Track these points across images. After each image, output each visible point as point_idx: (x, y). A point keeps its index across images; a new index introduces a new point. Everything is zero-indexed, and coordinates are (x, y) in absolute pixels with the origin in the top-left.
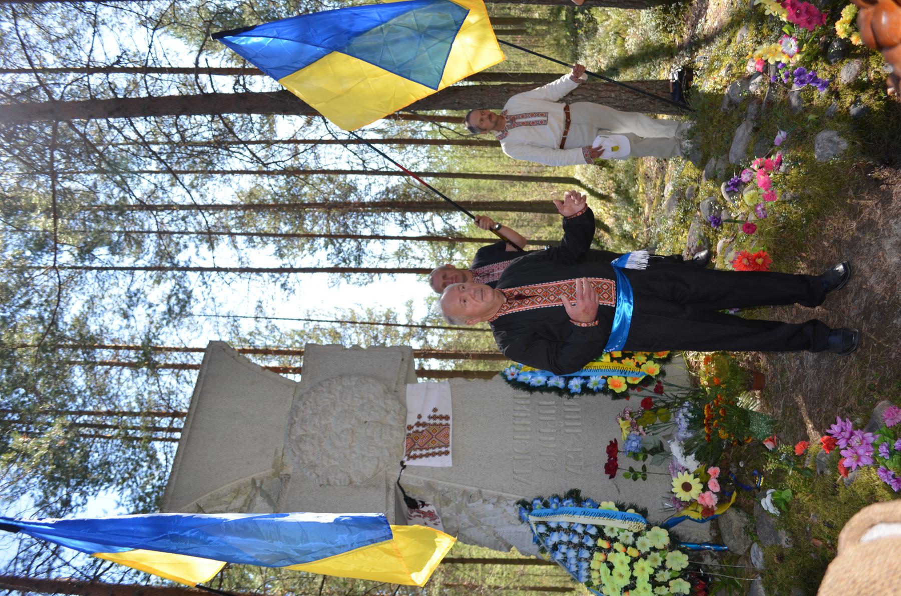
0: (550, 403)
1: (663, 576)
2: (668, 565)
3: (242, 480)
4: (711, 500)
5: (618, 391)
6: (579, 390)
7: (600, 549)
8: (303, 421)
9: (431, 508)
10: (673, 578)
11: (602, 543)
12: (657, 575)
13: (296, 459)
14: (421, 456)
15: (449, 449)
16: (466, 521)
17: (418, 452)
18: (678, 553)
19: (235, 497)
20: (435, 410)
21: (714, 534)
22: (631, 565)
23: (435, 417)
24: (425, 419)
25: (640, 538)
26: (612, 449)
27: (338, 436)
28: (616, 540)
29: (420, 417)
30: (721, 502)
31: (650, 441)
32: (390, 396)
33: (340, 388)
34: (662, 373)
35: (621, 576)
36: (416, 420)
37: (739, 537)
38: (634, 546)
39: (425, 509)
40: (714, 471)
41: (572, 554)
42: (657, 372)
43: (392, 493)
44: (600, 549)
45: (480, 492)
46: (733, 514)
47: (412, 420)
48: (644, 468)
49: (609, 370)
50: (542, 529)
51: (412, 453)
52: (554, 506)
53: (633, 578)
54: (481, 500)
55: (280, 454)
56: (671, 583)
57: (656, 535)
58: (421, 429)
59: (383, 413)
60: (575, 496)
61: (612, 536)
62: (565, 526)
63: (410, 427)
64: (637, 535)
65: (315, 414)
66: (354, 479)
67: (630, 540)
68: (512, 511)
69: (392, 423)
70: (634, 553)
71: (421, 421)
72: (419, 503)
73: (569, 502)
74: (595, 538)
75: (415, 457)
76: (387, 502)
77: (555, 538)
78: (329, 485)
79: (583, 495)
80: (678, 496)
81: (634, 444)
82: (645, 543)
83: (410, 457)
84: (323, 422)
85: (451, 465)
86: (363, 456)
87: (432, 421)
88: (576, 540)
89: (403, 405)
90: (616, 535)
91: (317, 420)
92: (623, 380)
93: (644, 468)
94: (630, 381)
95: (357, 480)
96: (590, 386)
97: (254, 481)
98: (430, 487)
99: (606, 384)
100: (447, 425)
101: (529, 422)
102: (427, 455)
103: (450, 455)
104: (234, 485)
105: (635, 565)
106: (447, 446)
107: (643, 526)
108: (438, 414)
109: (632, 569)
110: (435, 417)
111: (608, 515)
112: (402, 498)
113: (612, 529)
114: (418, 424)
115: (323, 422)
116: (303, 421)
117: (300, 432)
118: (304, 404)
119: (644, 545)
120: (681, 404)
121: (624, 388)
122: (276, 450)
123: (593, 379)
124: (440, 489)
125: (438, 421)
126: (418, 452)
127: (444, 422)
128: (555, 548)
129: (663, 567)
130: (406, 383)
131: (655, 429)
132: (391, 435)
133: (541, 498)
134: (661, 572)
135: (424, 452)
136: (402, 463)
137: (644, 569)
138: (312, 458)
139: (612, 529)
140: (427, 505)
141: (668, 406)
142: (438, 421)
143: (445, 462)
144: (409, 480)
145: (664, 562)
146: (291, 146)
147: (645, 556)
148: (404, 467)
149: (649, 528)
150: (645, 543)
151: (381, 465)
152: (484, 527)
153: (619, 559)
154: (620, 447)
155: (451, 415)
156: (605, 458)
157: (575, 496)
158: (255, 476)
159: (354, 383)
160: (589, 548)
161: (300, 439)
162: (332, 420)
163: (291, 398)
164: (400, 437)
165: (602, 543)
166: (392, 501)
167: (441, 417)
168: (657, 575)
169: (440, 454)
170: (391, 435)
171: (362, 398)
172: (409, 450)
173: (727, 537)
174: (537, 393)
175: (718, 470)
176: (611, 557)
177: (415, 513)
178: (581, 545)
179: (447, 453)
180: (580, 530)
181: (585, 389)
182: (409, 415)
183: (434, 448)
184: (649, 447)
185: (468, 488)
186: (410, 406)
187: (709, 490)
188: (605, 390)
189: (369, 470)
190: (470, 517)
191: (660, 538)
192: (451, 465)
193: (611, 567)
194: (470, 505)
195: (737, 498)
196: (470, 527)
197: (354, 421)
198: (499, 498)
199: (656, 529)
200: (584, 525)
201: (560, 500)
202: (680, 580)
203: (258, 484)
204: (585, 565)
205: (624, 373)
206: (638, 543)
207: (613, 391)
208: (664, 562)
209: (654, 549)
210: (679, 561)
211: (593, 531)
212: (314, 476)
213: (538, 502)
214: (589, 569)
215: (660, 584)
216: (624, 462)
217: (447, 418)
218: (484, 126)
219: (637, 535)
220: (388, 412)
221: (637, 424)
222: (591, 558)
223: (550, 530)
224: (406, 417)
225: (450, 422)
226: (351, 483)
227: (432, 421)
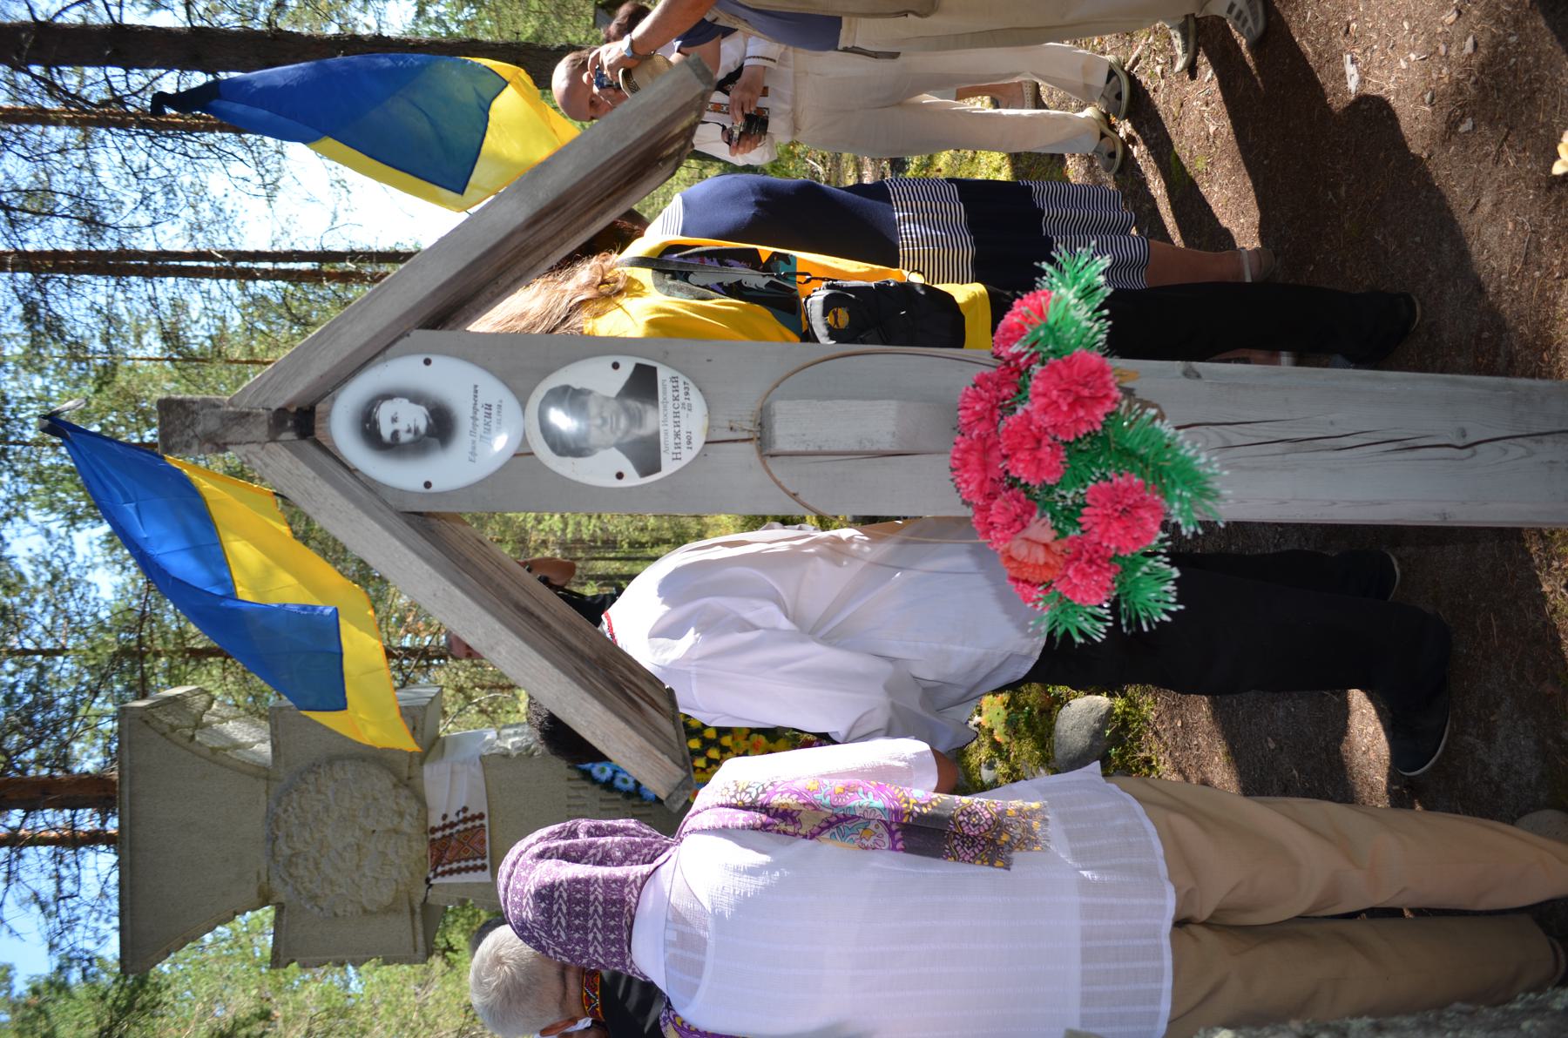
15: (487, 861)
20: (465, 809)
23: (465, 820)
24: (452, 818)
27: (340, 855)
32: (405, 792)
36: (441, 823)
51: (440, 869)
55: (264, 879)
59: (396, 820)
63: (434, 830)
65: (303, 825)
69: (409, 830)
75: (443, 874)
76: (414, 928)
86: (377, 879)
91: (307, 835)
100: (482, 826)
108: (468, 814)
110: (465, 820)
114: (444, 828)
117: (288, 852)
118: (286, 811)
122: (259, 874)
125: (469, 825)
127: (478, 823)
130: (422, 764)
132: (410, 848)
136: (428, 880)
142: (469, 825)
155: (486, 813)
159: (349, 776)
161: (290, 863)
163: (263, 797)
164: (422, 848)
167: (473, 818)
169: (475, 868)
170: (410, 848)
171: (364, 797)
172: (437, 863)
174: (597, 787)
179: (483, 868)
182: (431, 814)
183: (467, 860)
186: (430, 801)
189: (386, 895)
197: (358, 833)
212: (316, 909)
217: (481, 816)
220: (401, 815)
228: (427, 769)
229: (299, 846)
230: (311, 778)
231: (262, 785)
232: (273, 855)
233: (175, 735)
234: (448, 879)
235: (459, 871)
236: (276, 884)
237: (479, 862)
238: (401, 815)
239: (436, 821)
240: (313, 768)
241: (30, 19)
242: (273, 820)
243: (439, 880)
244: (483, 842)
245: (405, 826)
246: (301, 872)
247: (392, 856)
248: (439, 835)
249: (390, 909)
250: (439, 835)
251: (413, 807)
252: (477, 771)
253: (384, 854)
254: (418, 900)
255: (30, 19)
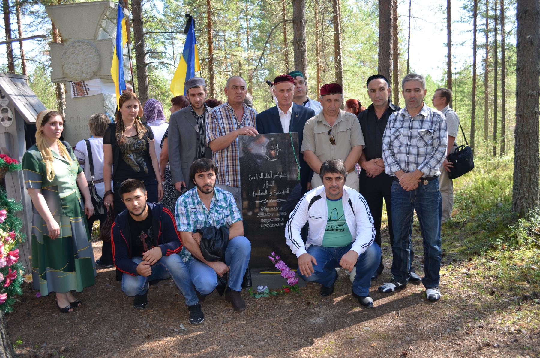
23: (86, 90)
24: (87, 87)
63: (84, 82)
65: (83, 49)
89: (91, 79)
161: (73, 46)
164: (79, 79)
169: (74, 93)
179: (75, 96)
186: (91, 81)
189: (67, 71)
217: (88, 94)
220: (87, 74)
228: (99, 79)
229: (77, 49)
230: (94, 50)
231: (92, 38)
233: (103, 15)
234: (72, 87)
235: (74, 89)
236: (69, 43)
238: (87, 74)
239: (86, 83)
240: (97, 51)
242: (83, 42)
244: (81, 95)
245: (84, 75)
246: (71, 50)
247: (76, 72)
248: (82, 84)
249: (64, 73)
250: (82, 84)
251: (89, 77)
252: (99, 93)
253: (77, 70)
254: (66, 79)
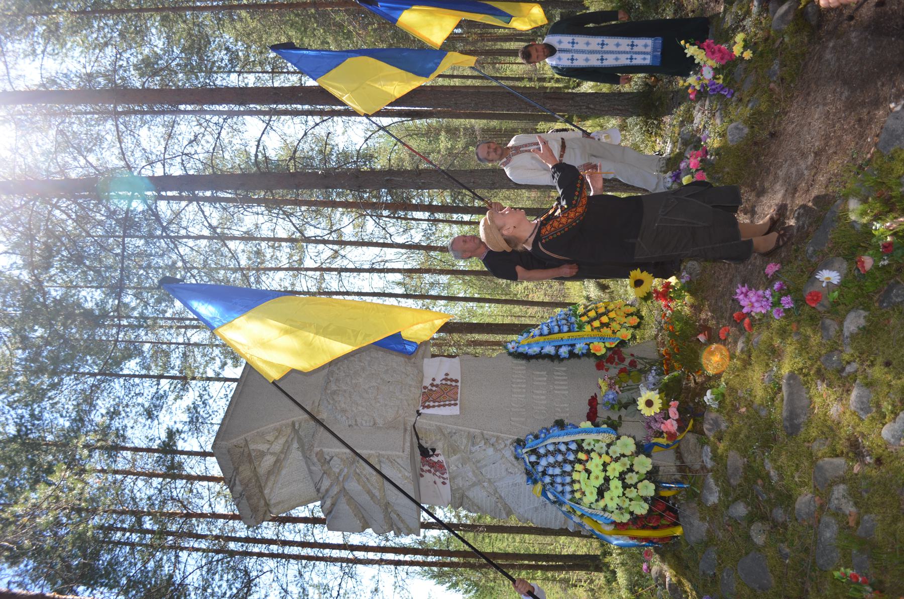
0: (542, 373)
1: (631, 478)
2: (636, 468)
3: (284, 422)
4: (671, 425)
5: (598, 354)
6: (567, 355)
7: (580, 461)
8: (337, 380)
9: (441, 458)
10: (641, 481)
11: (582, 456)
12: (627, 477)
13: (330, 407)
14: (434, 407)
15: (458, 402)
16: (470, 474)
17: (431, 404)
18: (642, 457)
19: (276, 438)
20: (447, 374)
21: (678, 463)
22: (605, 465)
23: (446, 379)
25: (612, 448)
26: (593, 402)
28: (593, 450)
29: (434, 380)
30: (681, 429)
31: (625, 397)
33: (368, 358)
34: (634, 337)
35: (597, 478)
37: (695, 451)
38: (607, 453)
39: (435, 459)
40: (674, 404)
41: (557, 471)
42: (629, 337)
43: (408, 433)
44: (580, 461)
45: (482, 434)
46: (690, 436)
47: (427, 382)
48: (620, 417)
49: (591, 338)
50: (533, 458)
51: (427, 404)
52: (543, 435)
53: (607, 479)
54: (483, 442)
56: (640, 485)
57: (626, 445)
58: (434, 388)
60: (560, 424)
61: (589, 448)
62: (551, 448)
63: (425, 388)
64: (609, 446)
66: (378, 421)
67: (605, 449)
68: (508, 453)
70: (607, 459)
71: (435, 383)
72: (431, 453)
73: (556, 431)
74: (576, 452)
75: (428, 407)
76: (404, 439)
77: (543, 462)
78: (357, 425)
79: (566, 421)
80: (642, 412)
81: (611, 396)
82: (616, 450)
83: (424, 407)
84: (354, 381)
85: (458, 413)
86: (386, 405)
87: (444, 382)
88: (560, 458)
90: (592, 446)
92: (602, 345)
93: (620, 417)
94: (608, 345)
95: (380, 422)
96: (576, 351)
97: (293, 424)
98: (440, 429)
99: (589, 349)
101: (524, 386)
102: (439, 406)
103: (458, 407)
104: (277, 424)
105: (608, 468)
106: (456, 400)
107: (614, 437)
108: (449, 377)
109: (605, 470)
110: (446, 379)
111: (587, 431)
112: (416, 445)
113: (589, 444)
114: (432, 385)
115: (354, 381)
116: (337, 380)
117: (334, 387)
118: (339, 369)
119: (615, 452)
120: (650, 370)
121: (603, 351)
123: (578, 346)
124: (449, 430)
125: (449, 383)
126: (431, 404)
127: (454, 384)
128: (544, 473)
129: (631, 470)
130: (423, 358)
131: (629, 390)
132: (410, 391)
133: (531, 434)
134: (630, 474)
135: (437, 404)
136: (418, 411)
137: (615, 469)
138: (343, 405)
139: (589, 444)
140: (437, 455)
141: (641, 371)
142: (449, 383)
143: (455, 410)
144: (421, 422)
145: (632, 465)
146: (318, 273)
147: (617, 460)
148: (419, 414)
149: (618, 438)
150: (616, 450)
151: (401, 412)
152: (485, 484)
153: (595, 464)
154: (599, 401)
156: (587, 409)
157: (560, 424)
158: (294, 419)
160: (572, 463)
162: (361, 380)
164: (418, 392)
165: (582, 456)
166: (408, 438)
167: (452, 380)
168: (627, 477)
169: (450, 405)
170: (410, 391)
173: (686, 455)
174: (533, 361)
175: (677, 403)
176: (589, 465)
177: (426, 468)
178: (565, 461)
179: (456, 404)
180: (563, 448)
181: (572, 355)
184: (624, 401)
185: (472, 430)
187: (669, 418)
188: (588, 354)
190: (474, 472)
191: (627, 445)
192: (458, 413)
193: (589, 472)
194: (473, 449)
195: (693, 426)
196: (474, 485)
198: (498, 438)
199: (624, 439)
200: (566, 444)
201: (548, 430)
202: (646, 482)
203: (297, 426)
204: (568, 479)
205: (603, 339)
206: (610, 452)
207: (594, 355)
208: (632, 465)
209: (624, 455)
210: (644, 464)
211: (573, 446)
212: (344, 418)
213: (531, 437)
214: (573, 482)
215: (630, 486)
216: (603, 413)
217: (456, 381)
218: (490, 158)
219: (609, 446)
221: (615, 384)
222: (573, 470)
223: (539, 456)
224: (422, 380)
225: (459, 384)
226: (375, 424)
227: (444, 382)
232: (326, 389)
237: (453, 402)
241: (234, 385)
243: (426, 411)
255: (234, 385)
